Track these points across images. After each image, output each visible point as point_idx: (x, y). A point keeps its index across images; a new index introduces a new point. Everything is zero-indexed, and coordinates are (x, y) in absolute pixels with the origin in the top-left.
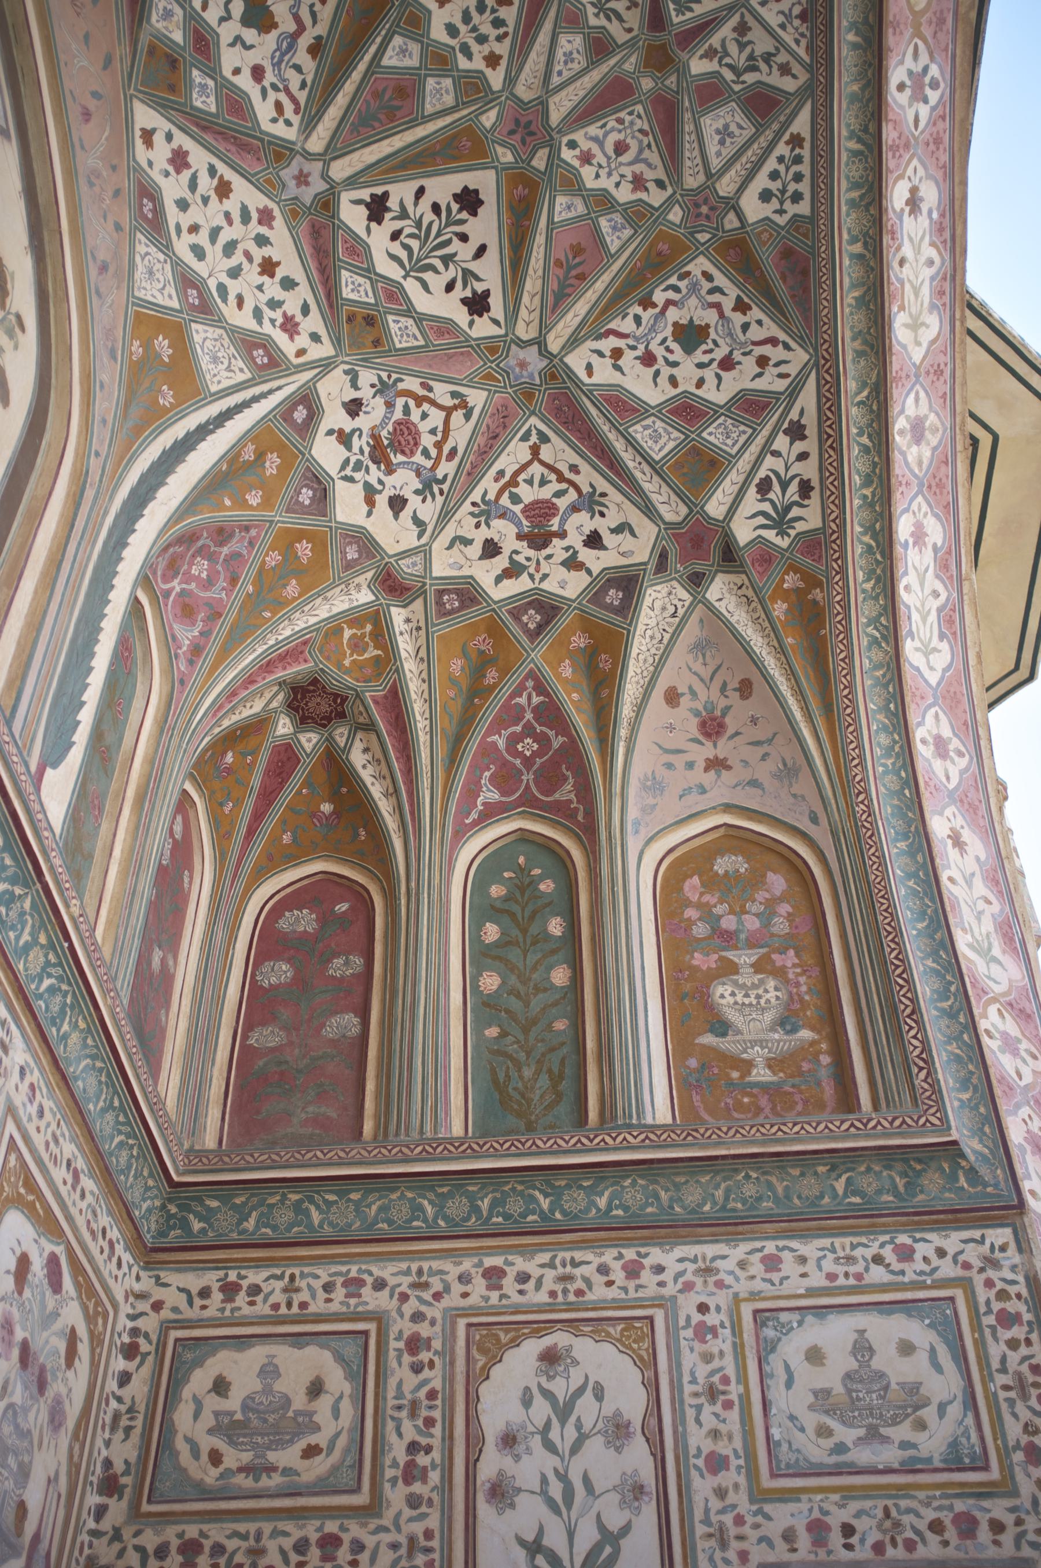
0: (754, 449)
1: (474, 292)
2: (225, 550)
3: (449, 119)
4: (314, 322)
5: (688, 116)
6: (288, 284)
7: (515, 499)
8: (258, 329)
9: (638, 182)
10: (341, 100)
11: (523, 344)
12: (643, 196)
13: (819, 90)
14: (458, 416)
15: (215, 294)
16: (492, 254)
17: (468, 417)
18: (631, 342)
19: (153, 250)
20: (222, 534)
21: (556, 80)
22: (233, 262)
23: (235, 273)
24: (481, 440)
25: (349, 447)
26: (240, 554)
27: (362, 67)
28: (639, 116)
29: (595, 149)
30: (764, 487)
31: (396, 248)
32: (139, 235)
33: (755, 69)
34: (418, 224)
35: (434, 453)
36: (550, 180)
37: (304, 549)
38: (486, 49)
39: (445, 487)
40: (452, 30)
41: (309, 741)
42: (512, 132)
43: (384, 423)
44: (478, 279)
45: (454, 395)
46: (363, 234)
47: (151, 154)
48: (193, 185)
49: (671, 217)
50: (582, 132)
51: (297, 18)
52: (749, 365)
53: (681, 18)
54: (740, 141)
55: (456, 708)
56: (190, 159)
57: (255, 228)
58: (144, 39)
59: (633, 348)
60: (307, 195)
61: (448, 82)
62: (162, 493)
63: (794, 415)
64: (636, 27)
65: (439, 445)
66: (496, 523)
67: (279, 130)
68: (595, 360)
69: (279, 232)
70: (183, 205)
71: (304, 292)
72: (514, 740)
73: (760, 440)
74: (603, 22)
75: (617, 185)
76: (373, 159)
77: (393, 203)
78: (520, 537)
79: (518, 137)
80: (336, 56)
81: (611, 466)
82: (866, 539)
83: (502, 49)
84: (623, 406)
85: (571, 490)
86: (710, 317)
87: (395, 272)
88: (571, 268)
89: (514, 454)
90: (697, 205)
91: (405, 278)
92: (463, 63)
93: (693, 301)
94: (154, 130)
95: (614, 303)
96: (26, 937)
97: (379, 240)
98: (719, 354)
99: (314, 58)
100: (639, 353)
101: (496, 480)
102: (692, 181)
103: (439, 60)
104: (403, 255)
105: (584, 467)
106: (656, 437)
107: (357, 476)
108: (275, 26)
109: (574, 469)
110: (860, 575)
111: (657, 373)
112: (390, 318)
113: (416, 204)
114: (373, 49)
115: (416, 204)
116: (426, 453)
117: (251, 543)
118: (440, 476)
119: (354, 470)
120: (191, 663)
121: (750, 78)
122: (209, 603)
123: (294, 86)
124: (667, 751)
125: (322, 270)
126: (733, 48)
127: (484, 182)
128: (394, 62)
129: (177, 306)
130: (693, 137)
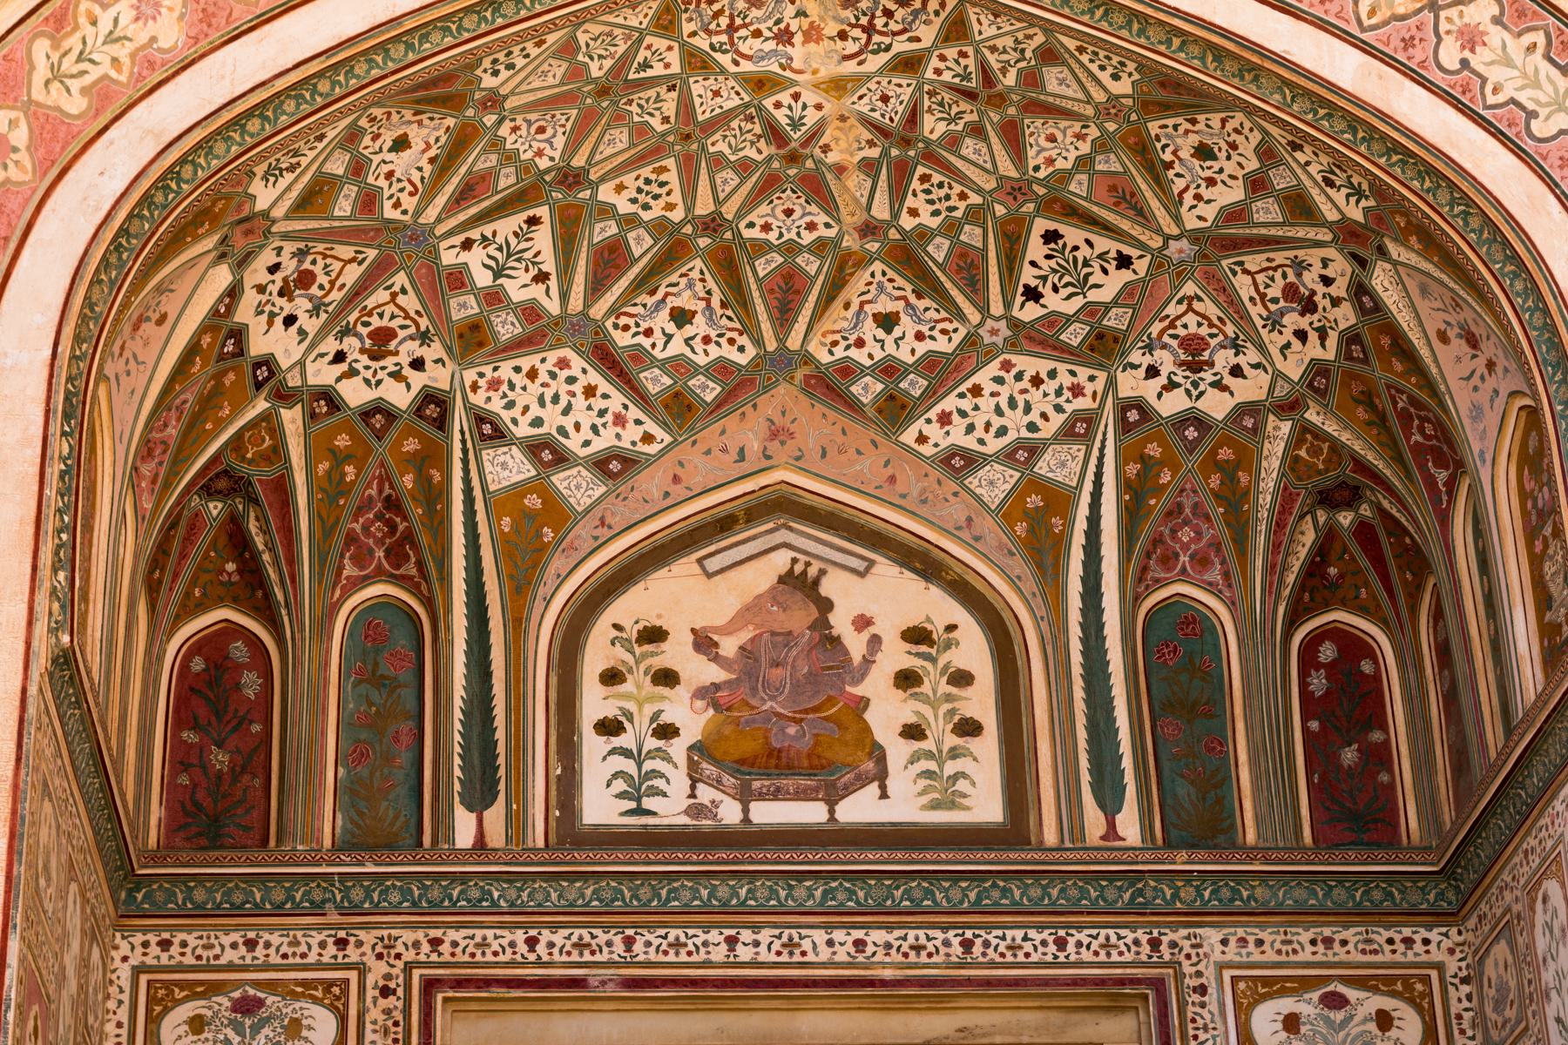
0: (1299, 171)
2: (1188, 511)
3: (991, 235)
4: (1083, 373)
6: (1052, 374)
7: (1275, 301)
10: (954, 292)
11: (1165, 245)
12: (1089, 139)
13: (1049, 28)
14: (1196, 305)
15: (1030, 435)
16: (1094, 238)
17: (1200, 299)
20: (1175, 511)
21: (989, 166)
22: (1021, 405)
24: (1222, 299)
25: (1178, 385)
27: (939, 273)
29: (1046, 154)
30: (1330, 183)
31: (1064, 292)
33: (1023, 51)
34: (1055, 271)
35: (1215, 331)
37: (1225, 454)
38: (954, 197)
40: (936, 213)
41: (1365, 510)
43: (1175, 355)
45: (1180, 302)
46: (1045, 311)
47: (931, 442)
48: (963, 414)
51: (898, 298)
52: (1239, 139)
54: (1070, 77)
55: (1384, 438)
57: (1009, 377)
58: (870, 412)
59: (1198, 186)
60: (1005, 332)
61: (967, 227)
63: (1284, 142)
65: (1211, 325)
66: (1285, 321)
67: (957, 338)
68: (1196, 212)
71: (1062, 368)
72: (1421, 430)
73: (1294, 165)
74: (962, 123)
77: (1033, 283)
78: (1302, 314)
80: (926, 284)
81: (1278, 243)
82: (1395, 158)
83: (957, 188)
84: (1234, 214)
86: (1194, 139)
87: (1078, 302)
92: (958, 214)
93: (1179, 141)
95: (1161, 185)
96: (1168, 893)
97: (1053, 302)
98: (1224, 147)
100: (1204, 185)
102: (1090, 111)
103: (951, 228)
104: (1071, 290)
105: (1271, 255)
106: (1267, 211)
107: (1202, 388)
110: (1416, 184)
116: (1212, 336)
117: (1195, 492)
120: (1230, 586)
121: (1028, 54)
122: (1209, 545)
123: (937, 316)
124: (1468, 378)
125: (1055, 348)
126: (1005, 57)
127: (1041, 225)
128: (943, 255)
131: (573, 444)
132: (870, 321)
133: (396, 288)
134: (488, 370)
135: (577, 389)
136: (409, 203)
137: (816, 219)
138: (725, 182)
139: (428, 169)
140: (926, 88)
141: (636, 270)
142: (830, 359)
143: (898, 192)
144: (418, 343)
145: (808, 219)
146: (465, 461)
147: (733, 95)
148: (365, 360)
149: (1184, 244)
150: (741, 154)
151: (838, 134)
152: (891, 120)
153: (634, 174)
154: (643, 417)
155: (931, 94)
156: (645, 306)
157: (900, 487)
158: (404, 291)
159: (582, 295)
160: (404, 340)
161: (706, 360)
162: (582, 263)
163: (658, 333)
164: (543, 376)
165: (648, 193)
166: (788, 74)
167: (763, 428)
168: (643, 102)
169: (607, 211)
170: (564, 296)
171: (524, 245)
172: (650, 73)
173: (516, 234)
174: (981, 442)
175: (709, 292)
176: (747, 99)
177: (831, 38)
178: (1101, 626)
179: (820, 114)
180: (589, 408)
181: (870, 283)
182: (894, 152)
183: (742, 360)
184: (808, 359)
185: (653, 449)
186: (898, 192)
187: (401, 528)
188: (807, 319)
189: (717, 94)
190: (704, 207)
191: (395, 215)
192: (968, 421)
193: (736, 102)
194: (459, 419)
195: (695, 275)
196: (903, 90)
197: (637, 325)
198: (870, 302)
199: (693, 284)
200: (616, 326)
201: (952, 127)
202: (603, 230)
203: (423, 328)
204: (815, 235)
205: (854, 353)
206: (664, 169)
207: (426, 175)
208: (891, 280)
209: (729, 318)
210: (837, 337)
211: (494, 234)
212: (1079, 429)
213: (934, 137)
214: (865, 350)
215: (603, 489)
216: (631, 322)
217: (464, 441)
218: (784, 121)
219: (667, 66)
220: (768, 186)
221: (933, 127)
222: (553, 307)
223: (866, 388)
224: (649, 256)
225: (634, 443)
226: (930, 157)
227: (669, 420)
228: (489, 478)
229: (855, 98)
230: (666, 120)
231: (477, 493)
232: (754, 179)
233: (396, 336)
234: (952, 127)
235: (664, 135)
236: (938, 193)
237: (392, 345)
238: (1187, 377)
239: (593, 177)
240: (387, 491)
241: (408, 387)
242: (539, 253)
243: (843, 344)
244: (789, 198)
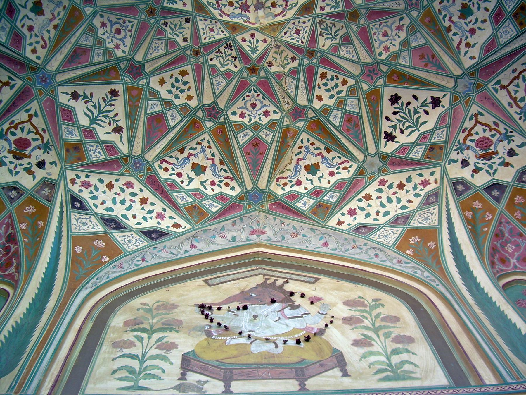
1: (431, 103)
2: (507, 235)
3: (362, 103)
4: (426, 174)
5: (377, 6)
6: (409, 180)
8: (422, 196)
9: (399, 28)
12: (405, 26)
14: (481, 119)
16: (417, 93)
17: (481, 114)
18: (464, 38)
19: (378, 233)
21: (355, 58)
22: (395, 200)
23: (399, 200)
25: (482, 169)
26: (511, 229)
27: (337, 134)
28: (374, 26)
29: (384, 45)
31: (407, 132)
32: (371, 237)
34: (400, 121)
36: (392, 65)
38: (340, 85)
39: (510, 130)
40: (331, 97)
42: (372, 78)
44: (426, 100)
45: (471, 119)
46: (398, 145)
47: (346, 223)
48: (362, 209)
49: (415, 16)
50: (376, 50)
51: (317, 155)
53: (341, 6)
56: (353, 208)
57: (385, 188)
62: (468, 259)
64: (342, 24)
65: (491, 129)
67: (352, 170)
69: (390, 178)
70: (368, 215)
71: (414, 174)
75: (399, 37)
76: (371, 135)
77: (389, 130)
79: (374, 76)
80: (332, 143)
83: (341, 78)
84: (491, 45)
85: (524, 74)
87: (416, 135)
88: (429, 61)
89: (503, 97)
90: (412, 4)
91: (419, 131)
92: (343, 94)
93: (451, 9)
94: (339, 220)
95: (446, 44)
97: (402, 139)
99: (331, 151)
100: (469, 35)
101: (512, 107)
103: (341, 103)
104: (410, 130)
105: (514, 67)
106: (507, 32)
107: (494, 168)
108: (318, 163)
109: (514, 71)
111: (479, 28)
112: (433, 140)
113: (392, 121)
114: (332, 128)
115: (392, 121)
116: (493, 136)
118: (504, 131)
119: (492, 169)
123: (340, 161)
127: (388, 92)
128: (338, 121)
129: (401, 229)
130: (385, 4)
131: (131, 222)
132: (303, 171)
133: (32, 112)
134: (83, 175)
135: (137, 199)
136: (42, 52)
137: (269, 109)
138: (218, 84)
139: (53, 32)
140: (318, 20)
141: (171, 135)
142: (283, 192)
143: (310, 86)
144: (42, 151)
145: (264, 109)
146: (61, 218)
147: (220, 32)
148: (10, 157)
149: (466, 80)
150: (226, 68)
151: (275, 55)
152: (302, 42)
153: (169, 73)
154: (174, 215)
155: (321, 23)
156: (177, 159)
157: (330, 246)
158: (36, 115)
159: (141, 144)
160: (34, 148)
161: (213, 193)
162: (141, 124)
163: (185, 176)
164: (116, 189)
165: (177, 88)
166: (247, 24)
167: (248, 231)
168: (173, 26)
169: (154, 95)
170: (131, 144)
171: (108, 108)
172: (175, 6)
173: (103, 99)
174: (375, 220)
175: (213, 155)
176: (227, 35)
177: (268, 8)
178: (478, 285)
179: (266, 45)
180: (143, 209)
181: (301, 147)
182: (306, 62)
183: (234, 193)
184: (270, 195)
185: (180, 230)
186: (310, 86)
187: (13, 250)
188: (268, 171)
189: (212, 30)
190: (208, 100)
191: (33, 57)
192: (365, 212)
193: (222, 36)
194: (60, 196)
195: (205, 144)
196: (306, 24)
197: (173, 170)
198: (302, 159)
199: (204, 147)
200: (160, 167)
201: (334, 42)
202: (153, 106)
203: (46, 141)
204: (269, 118)
205: (296, 188)
206: (184, 73)
207: (52, 36)
208: (312, 144)
209: (225, 171)
210: (286, 181)
211: (92, 94)
212: (432, 199)
213: (325, 48)
214: (302, 186)
215: (147, 243)
216: (169, 167)
217: (62, 208)
218: (247, 49)
219: (185, 5)
220: (242, 86)
221: (324, 43)
222: (124, 149)
223: (305, 203)
224: (179, 127)
225: (168, 227)
226: (325, 61)
227: (190, 218)
228: (73, 227)
229: (283, 34)
230: (185, 40)
231: (64, 233)
232: (234, 83)
233: (29, 145)
234: (334, 42)
235: (185, 49)
236: (332, 84)
237: (28, 151)
238: (485, 164)
239: (147, 70)
240: (10, 231)
241: (34, 178)
242: (116, 115)
243: (290, 184)
244: (254, 96)
